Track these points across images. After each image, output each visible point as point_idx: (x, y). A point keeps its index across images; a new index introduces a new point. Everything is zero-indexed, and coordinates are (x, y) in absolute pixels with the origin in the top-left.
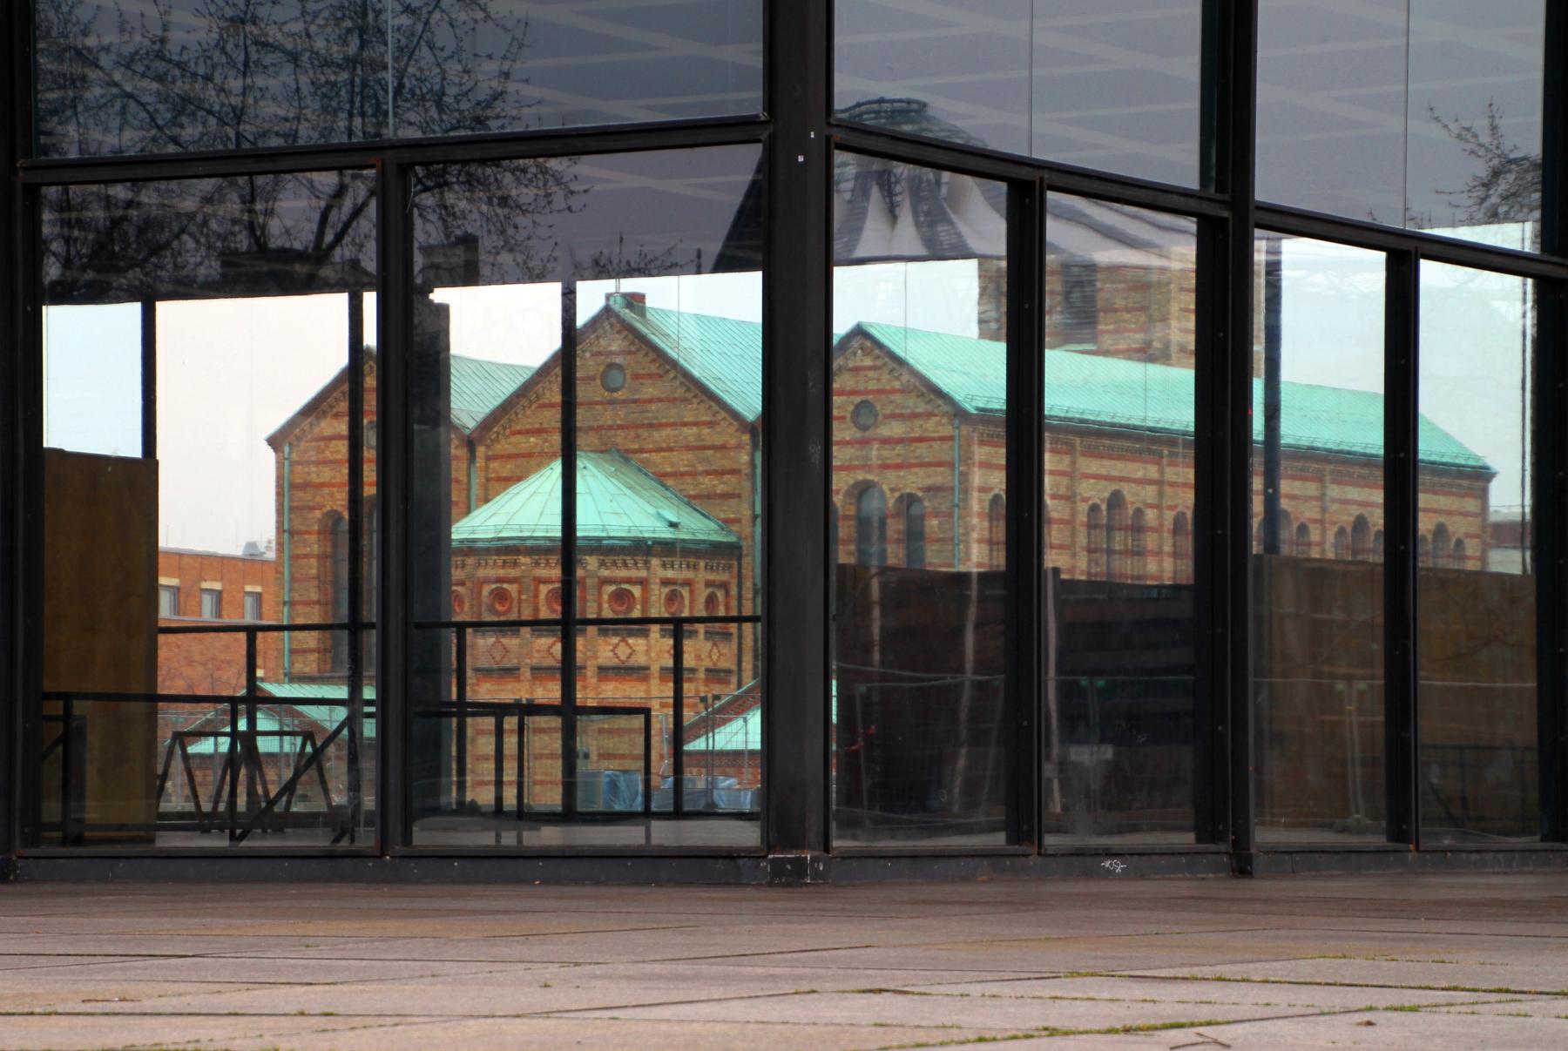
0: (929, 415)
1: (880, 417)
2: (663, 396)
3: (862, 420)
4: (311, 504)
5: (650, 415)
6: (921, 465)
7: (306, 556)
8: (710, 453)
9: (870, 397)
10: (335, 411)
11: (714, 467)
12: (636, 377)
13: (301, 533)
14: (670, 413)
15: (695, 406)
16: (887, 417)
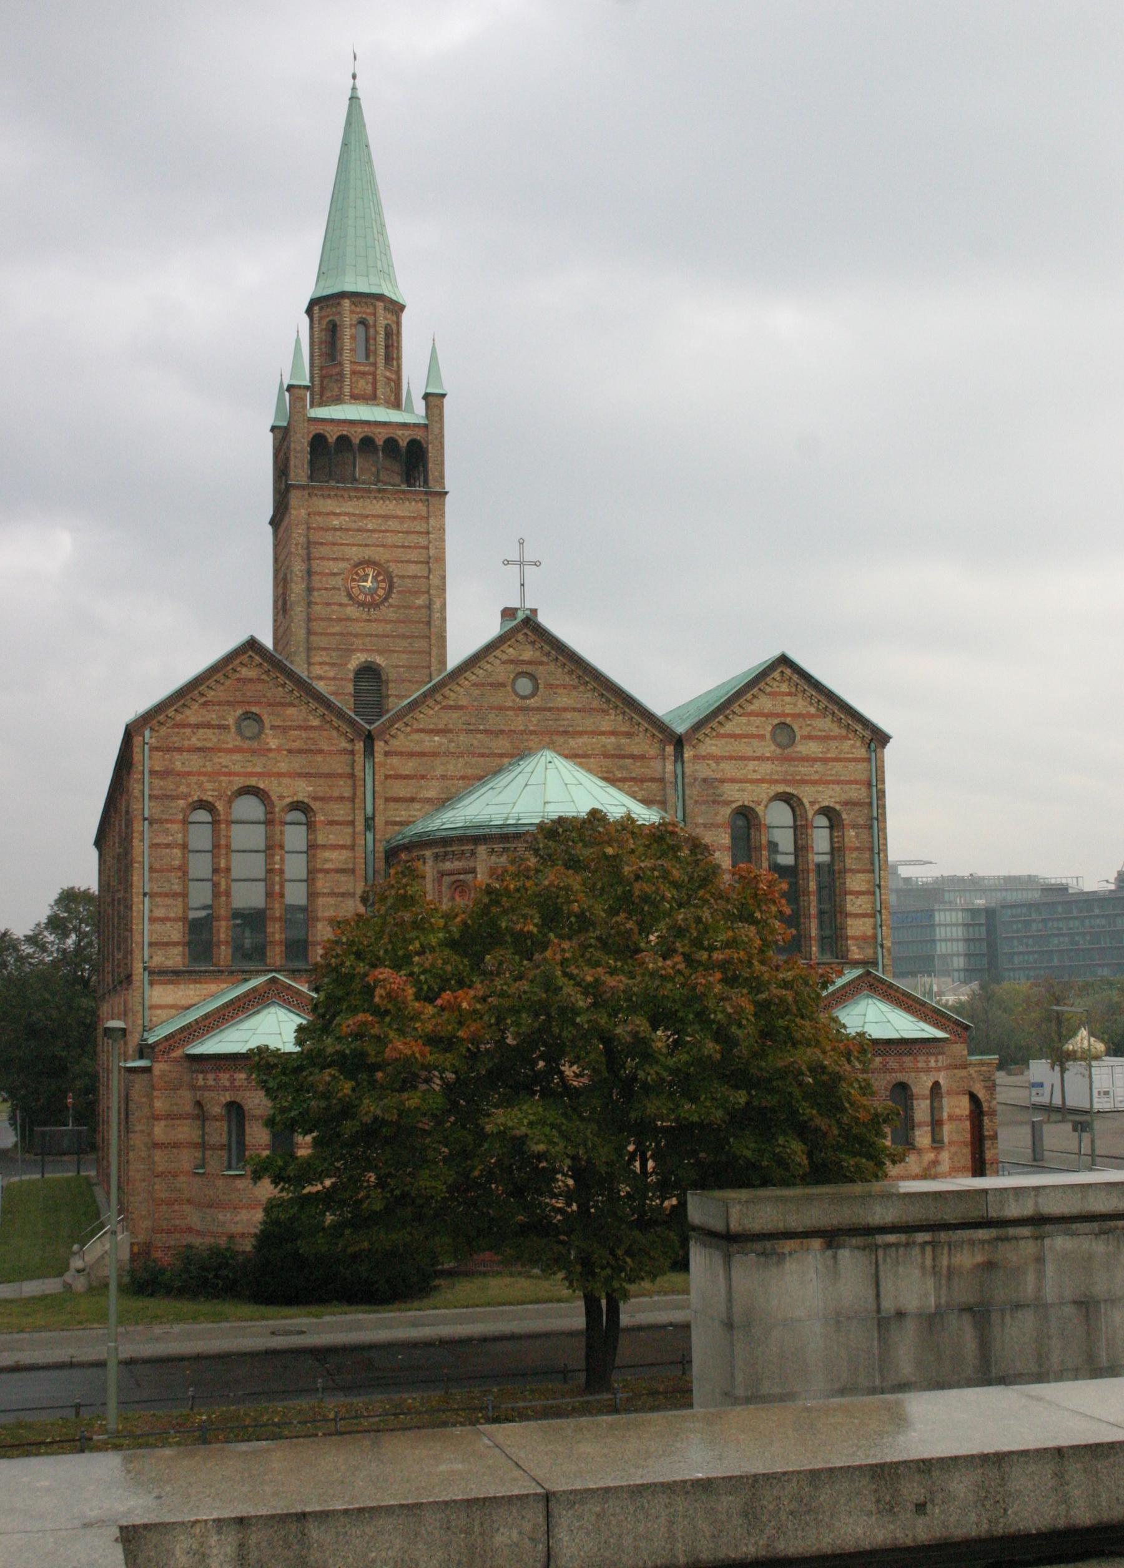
0: (846, 738)
1: (798, 738)
2: (579, 706)
3: (778, 740)
4: (174, 793)
5: (565, 723)
6: (838, 782)
7: (168, 846)
8: (628, 761)
9: (788, 720)
10: (204, 699)
11: (634, 775)
12: (550, 686)
13: (160, 821)
14: (589, 723)
15: (612, 717)
16: (804, 737)
